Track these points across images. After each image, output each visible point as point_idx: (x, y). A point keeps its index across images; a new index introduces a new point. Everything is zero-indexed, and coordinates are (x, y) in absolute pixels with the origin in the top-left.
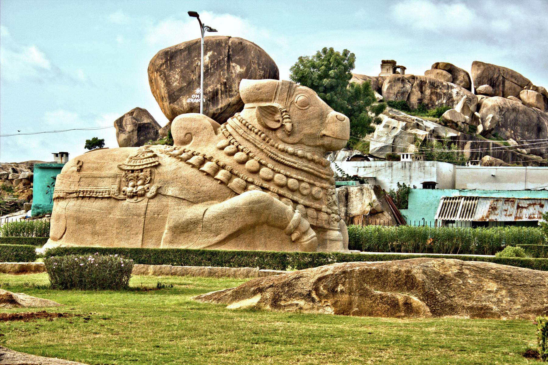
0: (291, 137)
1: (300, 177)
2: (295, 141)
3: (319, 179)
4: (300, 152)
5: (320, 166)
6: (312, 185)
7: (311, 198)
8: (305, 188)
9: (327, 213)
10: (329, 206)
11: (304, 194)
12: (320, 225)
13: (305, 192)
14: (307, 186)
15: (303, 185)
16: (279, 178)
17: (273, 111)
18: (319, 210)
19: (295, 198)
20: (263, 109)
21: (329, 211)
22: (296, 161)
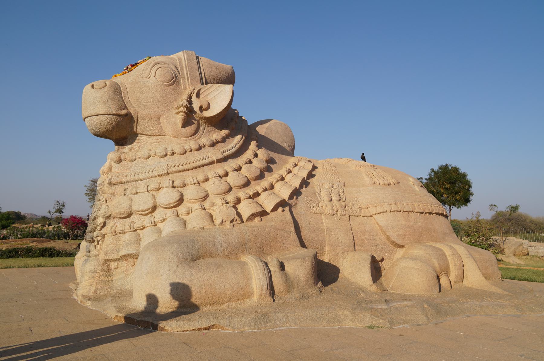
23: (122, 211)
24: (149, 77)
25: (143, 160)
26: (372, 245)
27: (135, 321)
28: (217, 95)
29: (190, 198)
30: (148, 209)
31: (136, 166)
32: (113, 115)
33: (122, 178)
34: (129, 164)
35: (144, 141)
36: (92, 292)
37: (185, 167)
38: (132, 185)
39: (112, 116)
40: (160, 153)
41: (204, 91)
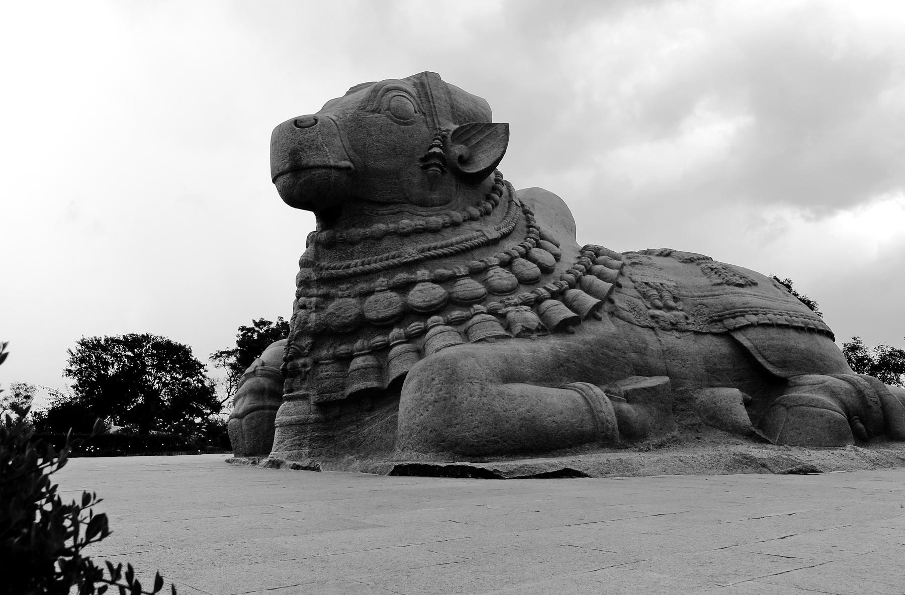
23: (347, 321)
24: (378, 110)
25: (374, 241)
26: (734, 378)
27: (438, 468)
28: (482, 139)
30: (393, 316)
31: (361, 251)
32: (330, 167)
33: (340, 270)
35: (371, 213)
36: (306, 454)
37: (445, 251)
38: (358, 280)
39: (328, 170)
40: (404, 228)
41: (462, 134)
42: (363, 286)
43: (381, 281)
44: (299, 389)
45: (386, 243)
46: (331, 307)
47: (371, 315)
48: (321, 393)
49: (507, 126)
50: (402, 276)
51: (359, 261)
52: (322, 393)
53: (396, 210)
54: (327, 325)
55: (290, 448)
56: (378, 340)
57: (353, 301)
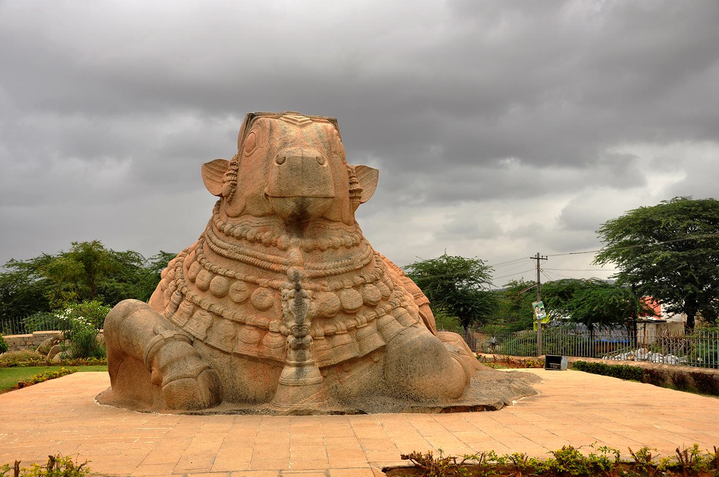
0: (233, 205)
1: (230, 273)
2: (238, 212)
3: (270, 273)
4: (237, 231)
5: (275, 250)
6: (255, 284)
7: (252, 307)
8: (239, 291)
9: (280, 332)
10: (284, 320)
11: (235, 300)
12: (267, 356)
13: (237, 297)
14: (243, 286)
15: (235, 285)
16: (203, 277)
17: (224, 168)
18: (265, 330)
19: (217, 308)
20: (210, 168)
21: (283, 328)
22: (226, 245)
29: (386, 295)
34: (321, 254)
42: (337, 283)
43: (347, 282)
44: (309, 358)
45: (340, 252)
46: (322, 296)
47: (348, 306)
48: (321, 361)
49: (378, 171)
50: (358, 280)
51: (330, 264)
52: (323, 361)
53: (338, 227)
54: (320, 311)
55: (316, 401)
56: (352, 323)
57: (333, 294)
